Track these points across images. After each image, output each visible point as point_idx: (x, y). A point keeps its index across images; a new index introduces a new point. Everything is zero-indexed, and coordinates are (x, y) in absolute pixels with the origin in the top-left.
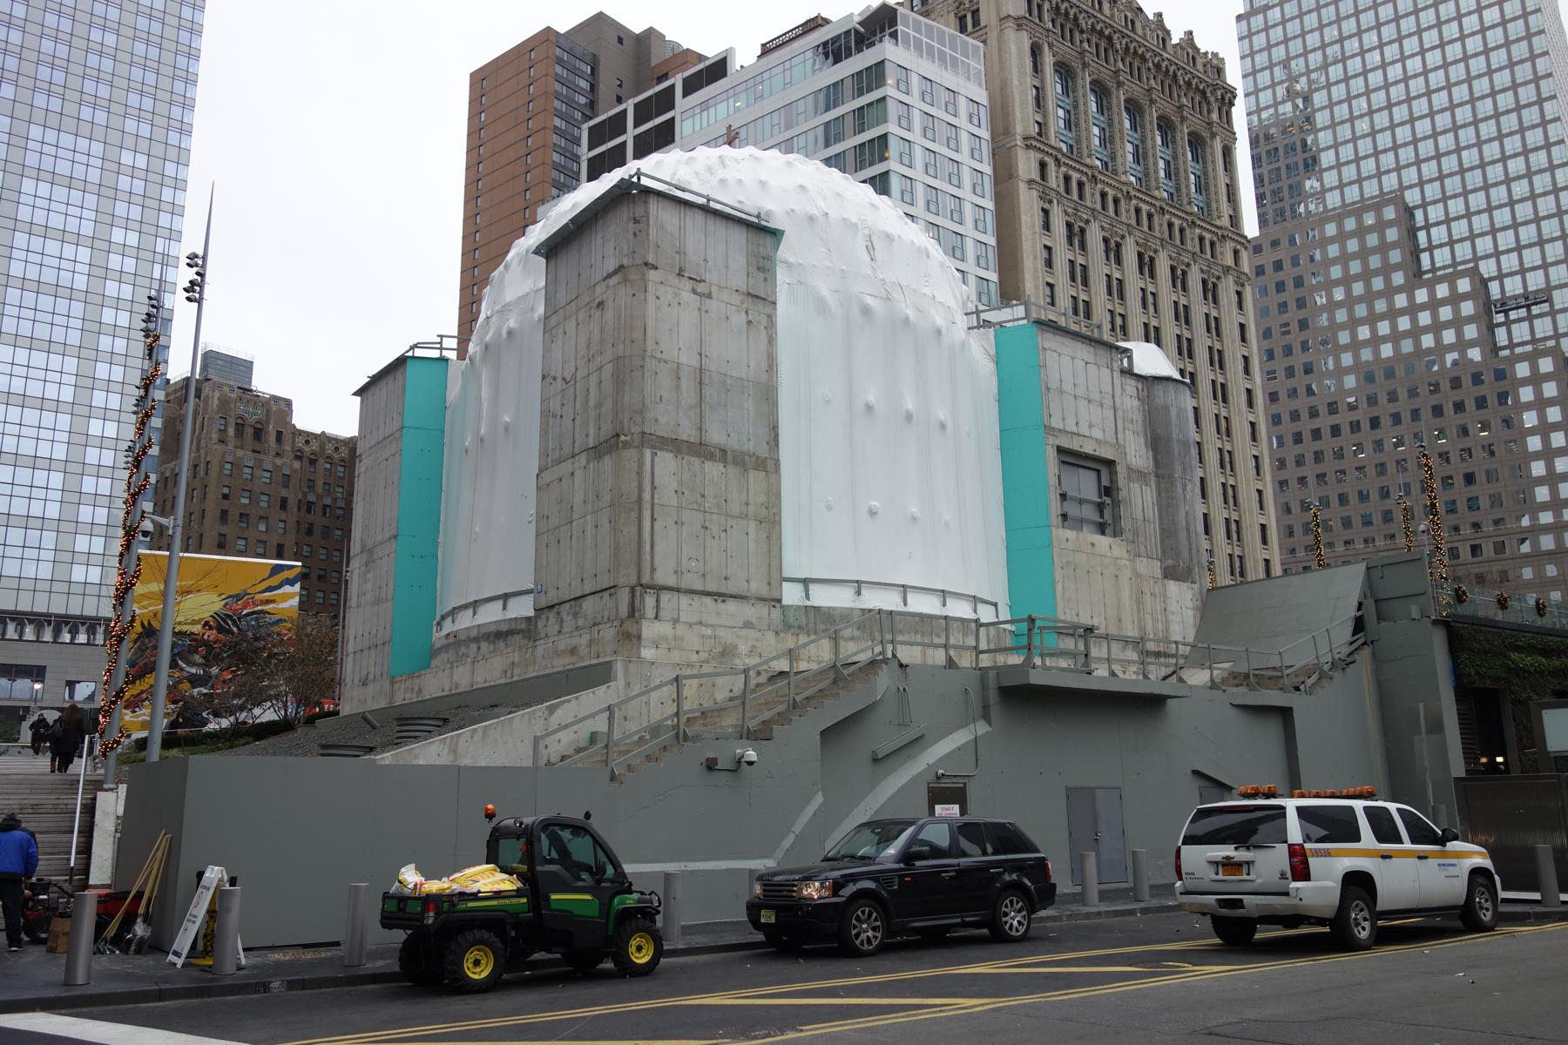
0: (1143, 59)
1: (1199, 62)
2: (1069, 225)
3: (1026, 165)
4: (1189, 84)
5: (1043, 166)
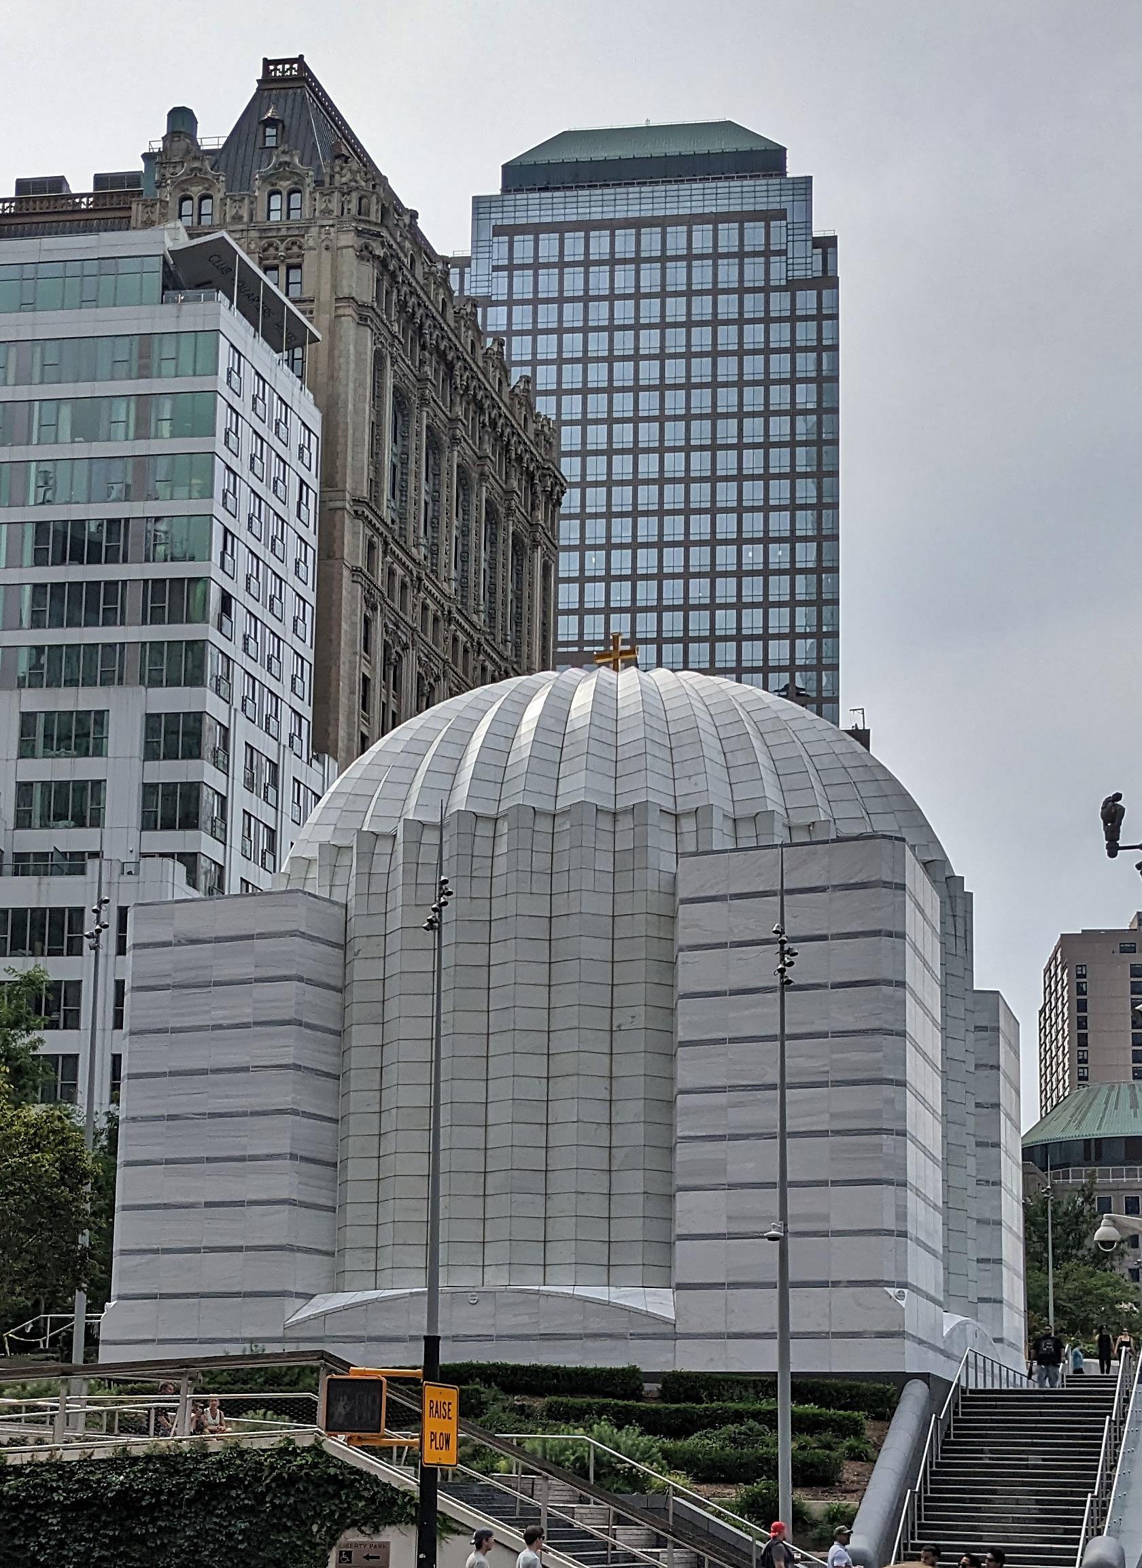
0: (480, 409)
1: (532, 427)
2: (386, 647)
3: (353, 541)
4: (519, 459)
5: (371, 546)
